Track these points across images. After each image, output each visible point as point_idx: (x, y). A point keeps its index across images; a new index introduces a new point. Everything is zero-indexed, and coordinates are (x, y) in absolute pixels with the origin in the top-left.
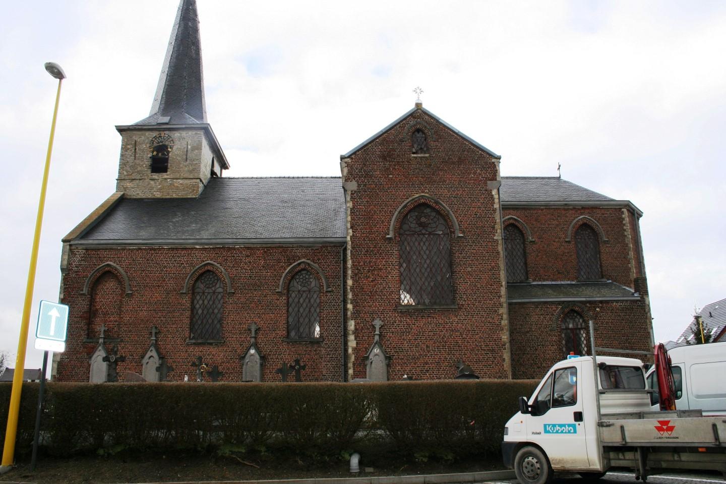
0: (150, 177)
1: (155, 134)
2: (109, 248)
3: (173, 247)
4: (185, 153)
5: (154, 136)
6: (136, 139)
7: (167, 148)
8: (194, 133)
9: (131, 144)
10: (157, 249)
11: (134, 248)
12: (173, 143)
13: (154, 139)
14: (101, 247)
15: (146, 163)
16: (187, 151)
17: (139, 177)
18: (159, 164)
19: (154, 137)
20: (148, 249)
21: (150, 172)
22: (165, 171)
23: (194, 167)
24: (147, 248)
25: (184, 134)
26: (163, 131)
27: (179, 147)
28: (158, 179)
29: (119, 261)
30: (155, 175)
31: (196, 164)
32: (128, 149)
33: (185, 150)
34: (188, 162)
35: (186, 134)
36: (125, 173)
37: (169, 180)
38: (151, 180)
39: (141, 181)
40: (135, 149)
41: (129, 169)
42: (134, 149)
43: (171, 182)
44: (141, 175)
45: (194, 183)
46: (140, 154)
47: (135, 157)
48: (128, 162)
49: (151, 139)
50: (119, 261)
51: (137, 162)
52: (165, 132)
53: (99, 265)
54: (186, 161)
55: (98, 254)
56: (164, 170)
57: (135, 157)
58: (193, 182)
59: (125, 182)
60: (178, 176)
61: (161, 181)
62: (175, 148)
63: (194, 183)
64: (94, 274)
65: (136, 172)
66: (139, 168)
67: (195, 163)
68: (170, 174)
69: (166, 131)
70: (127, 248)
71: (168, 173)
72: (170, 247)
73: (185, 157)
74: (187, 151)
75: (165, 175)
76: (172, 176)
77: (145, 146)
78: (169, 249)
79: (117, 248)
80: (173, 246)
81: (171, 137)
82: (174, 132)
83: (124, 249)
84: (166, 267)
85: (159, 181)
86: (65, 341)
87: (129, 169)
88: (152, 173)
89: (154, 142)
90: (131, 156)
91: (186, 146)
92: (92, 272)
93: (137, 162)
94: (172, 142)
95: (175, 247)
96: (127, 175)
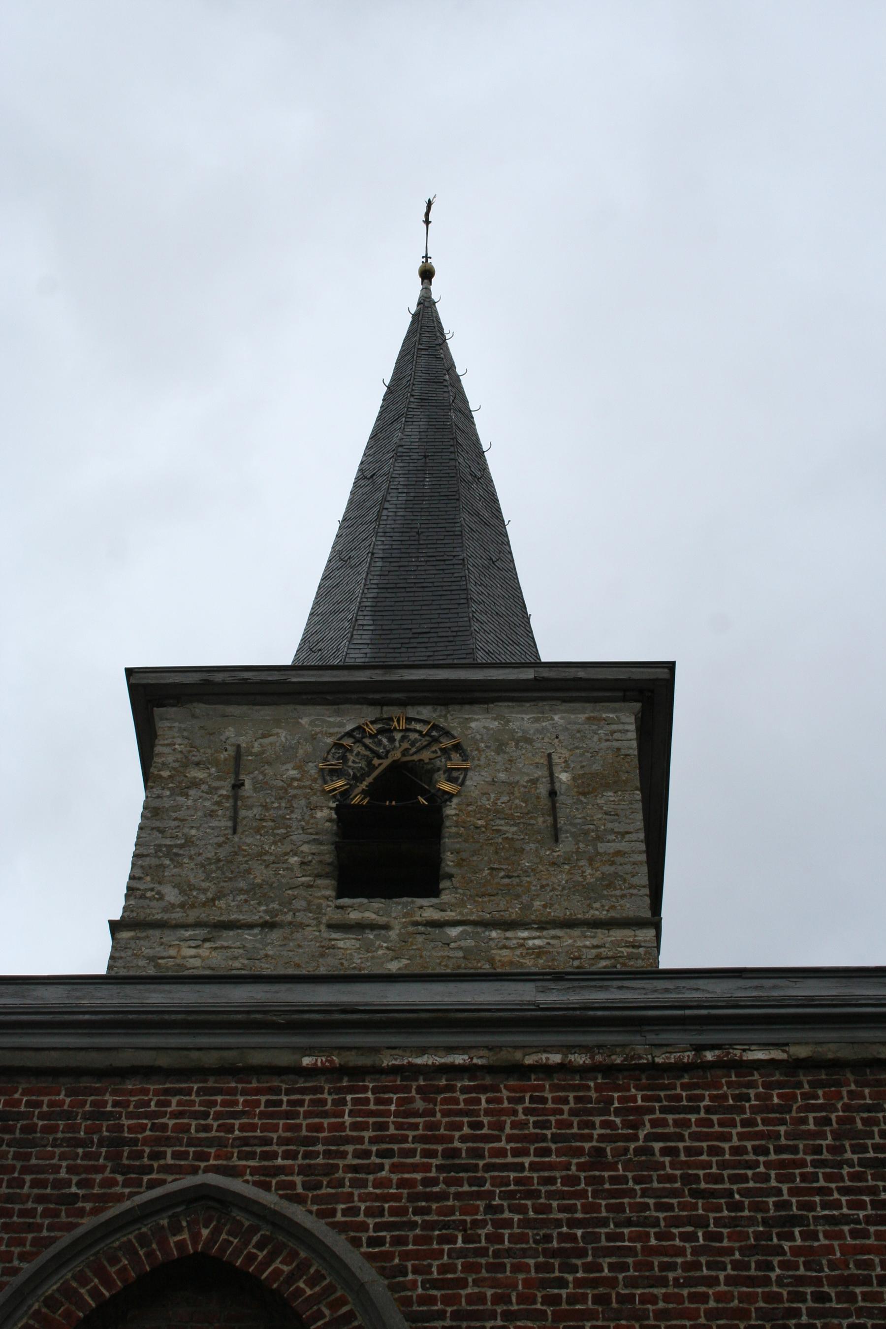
0: (331, 914)
1: (347, 720)
2: (211, 1059)
3: (830, 1052)
4: (545, 801)
5: (349, 727)
6: (243, 741)
7: (431, 782)
8: (582, 717)
9: (216, 763)
10: (681, 1068)
11: (459, 1059)
12: (465, 758)
13: (348, 742)
14: (132, 1049)
15: (305, 848)
16: (553, 793)
17: (260, 914)
18: (390, 839)
19: (349, 734)
20: (584, 1071)
21: (330, 893)
22: (435, 892)
23: (609, 869)
24: (579, 1059)
25: (522, 720)
26: (403, 704)
27: (502, 776)
28: (386, 927)
29: (304, 1170)
30: (360, 908)
31: (618, 853)
32: (195, 784)
33: (543, 789)
34: (566, 846)
35: (537, 720)
36: (172, 895)
37: (454, 932)
38: (331, 926)
39: (275, 935)
40: (238, 786)
41: (196, 878)
42: (230, 781)
43: (470, 943)
44: (275, 905)
45: (625, 951)
46: (265, 807)
47: (235, 818)
48: (189, 842)
49: (330, 741)
50: (304, 1170)
51: (250, 841)
52: (412, 712)
53: (105, 1200)
54: (556, 840)
55: (98, 1114)
56: (425, 880)
57: (235, 818)
58: (616, 944)
59: (169, 937)
60: (514, 912)
61: (404, 940)
62: (474, 780)
63: (625, 951)
64: (52, 1287)
65: (241, 891)
66: (260, 874)
67: (612, 847)
68: (462, 903)
69: (423, 702)
70: (387, 1061)
71: (445, 897)
72: (802, 1052)
73: (541, 822)
74: (553, 793)
75: (427, 909)
76: (471, 911)
77: (293, 773)
78: (796, 1065)
79: (284, 1059)
80: (832, 1044)
81: (447, 734)
82: (466, 712)
83: (357, 1073)
84: (794, 1221)
85: (393, 934)
86: (609, 930)
87: (196, 878)
88: (339, 896)
89: (351, 758)
90: (212, 814)
91: (542, 772)
92: (28, 1268)
93: (250, 841)
94: (455, 756)
95: (846, 1053)
96: (182, 906)
